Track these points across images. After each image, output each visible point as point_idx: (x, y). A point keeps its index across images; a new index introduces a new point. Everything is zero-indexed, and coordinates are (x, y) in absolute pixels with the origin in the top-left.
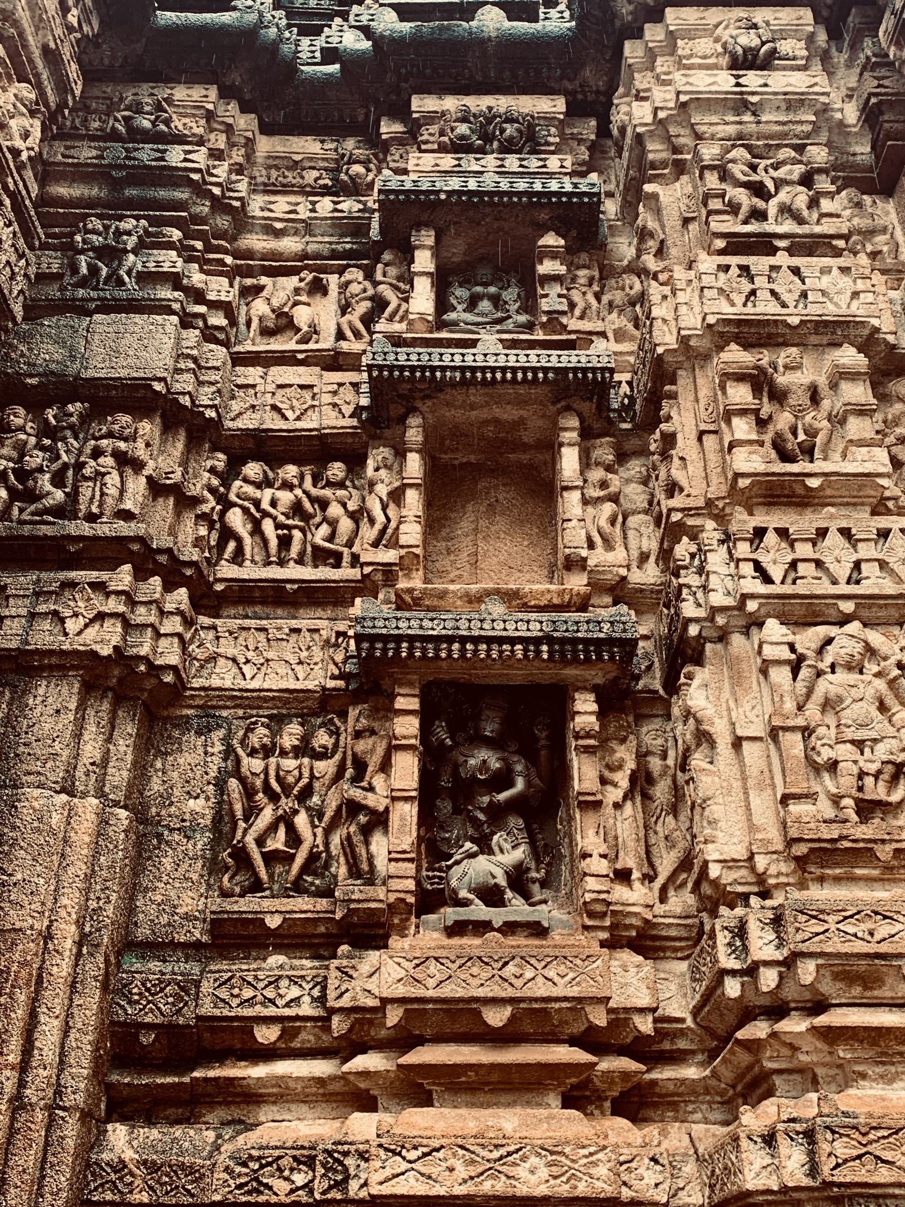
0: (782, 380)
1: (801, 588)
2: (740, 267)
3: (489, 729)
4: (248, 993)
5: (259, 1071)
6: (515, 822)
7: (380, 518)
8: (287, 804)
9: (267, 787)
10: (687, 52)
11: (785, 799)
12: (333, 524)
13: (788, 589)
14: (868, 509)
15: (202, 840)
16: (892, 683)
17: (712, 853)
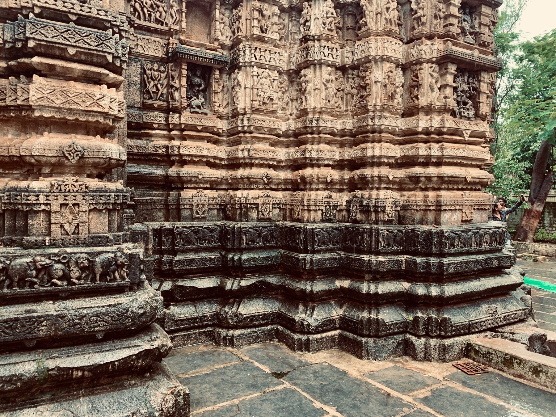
0: (265, 12)
1: (261, 62)
3: (198, 74)
4: (152, 118)
5: (154, 132)
6: (202, 93)
7: (175, 17)
8: (156, 82)
9: (152, 77)
11: (252, 101)
12: (161, 13)
13: (259, 61)
15: (138, 87)
16: (271, 82)
17: (239, 106)
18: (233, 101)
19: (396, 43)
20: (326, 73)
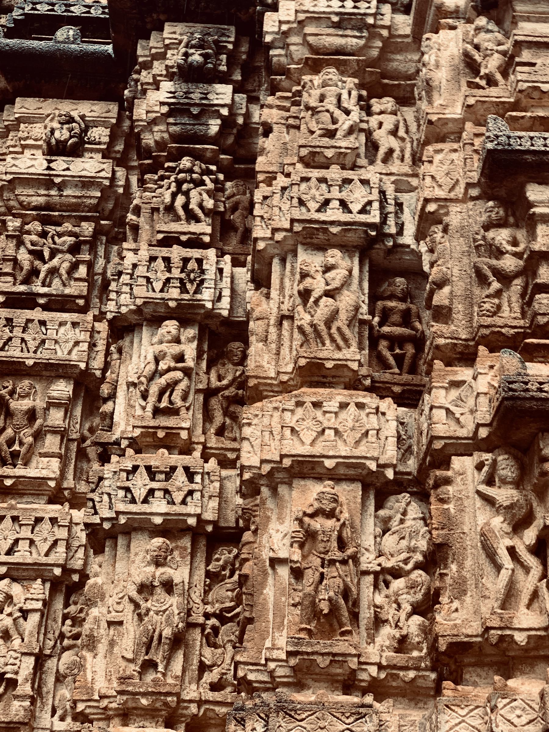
2: (7, 319)
10: (26, 134)
14: (46, 498)
19: (343, 406)
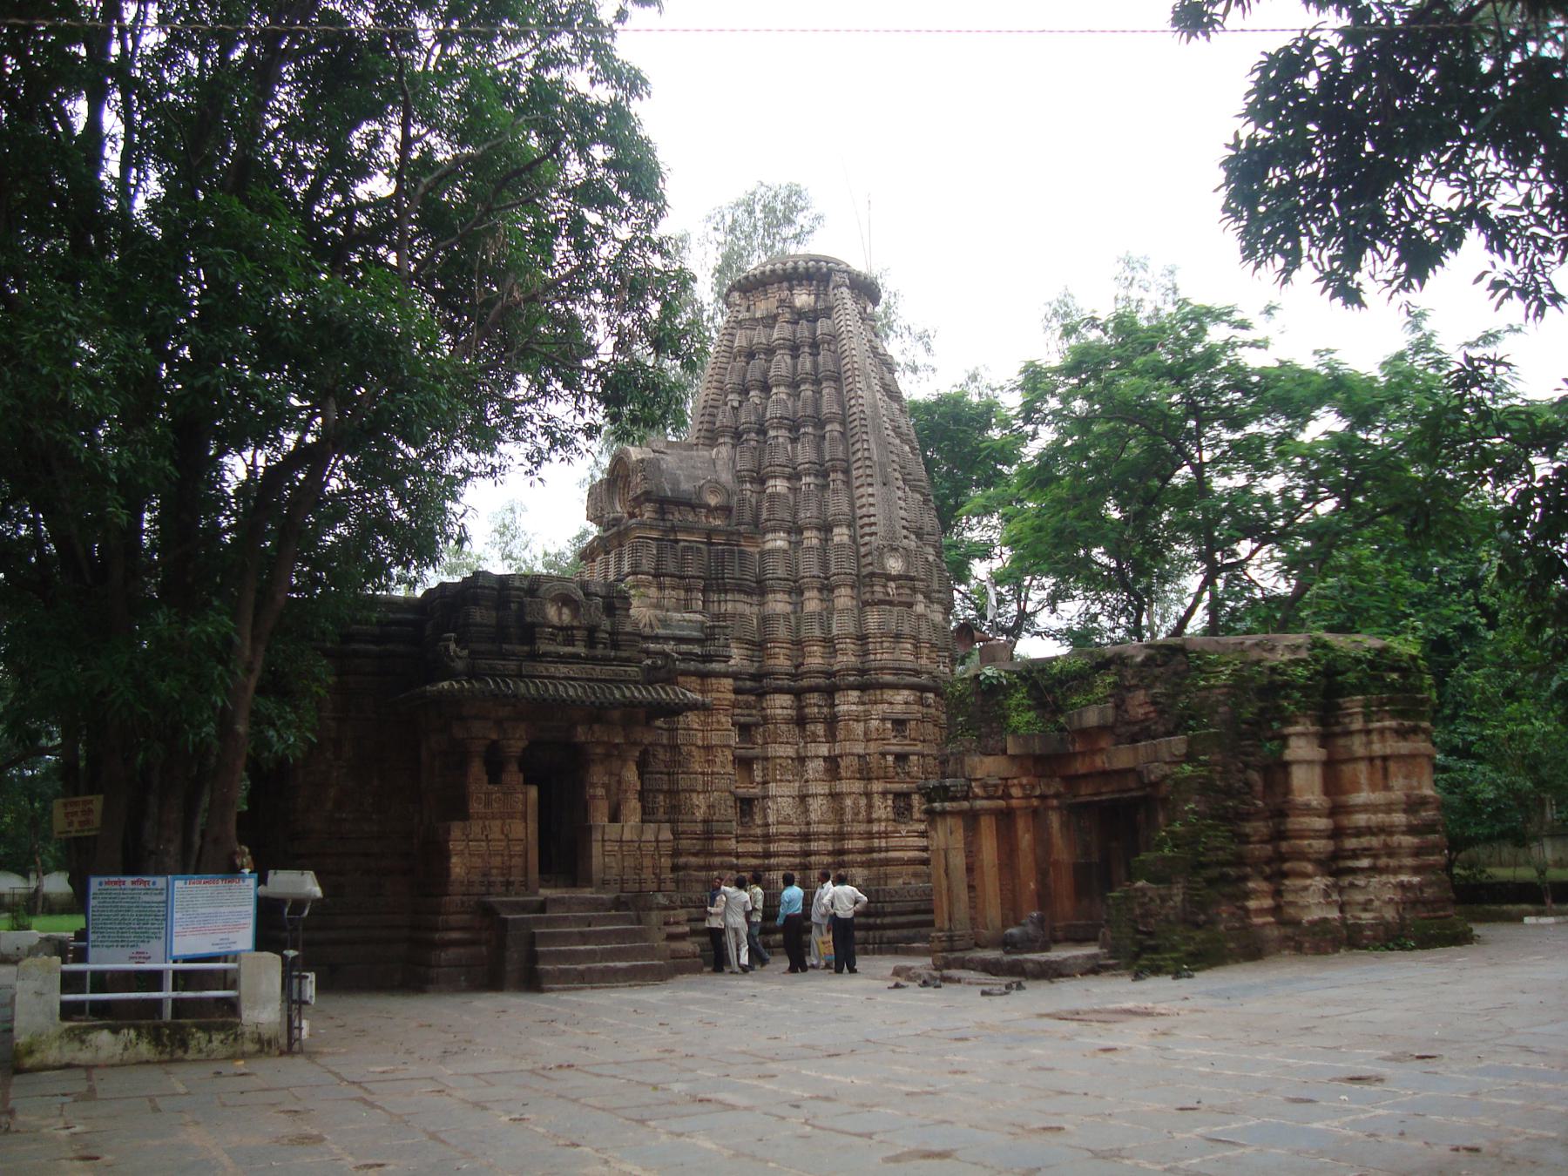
18: (765, 816)
20: (820, 800)
